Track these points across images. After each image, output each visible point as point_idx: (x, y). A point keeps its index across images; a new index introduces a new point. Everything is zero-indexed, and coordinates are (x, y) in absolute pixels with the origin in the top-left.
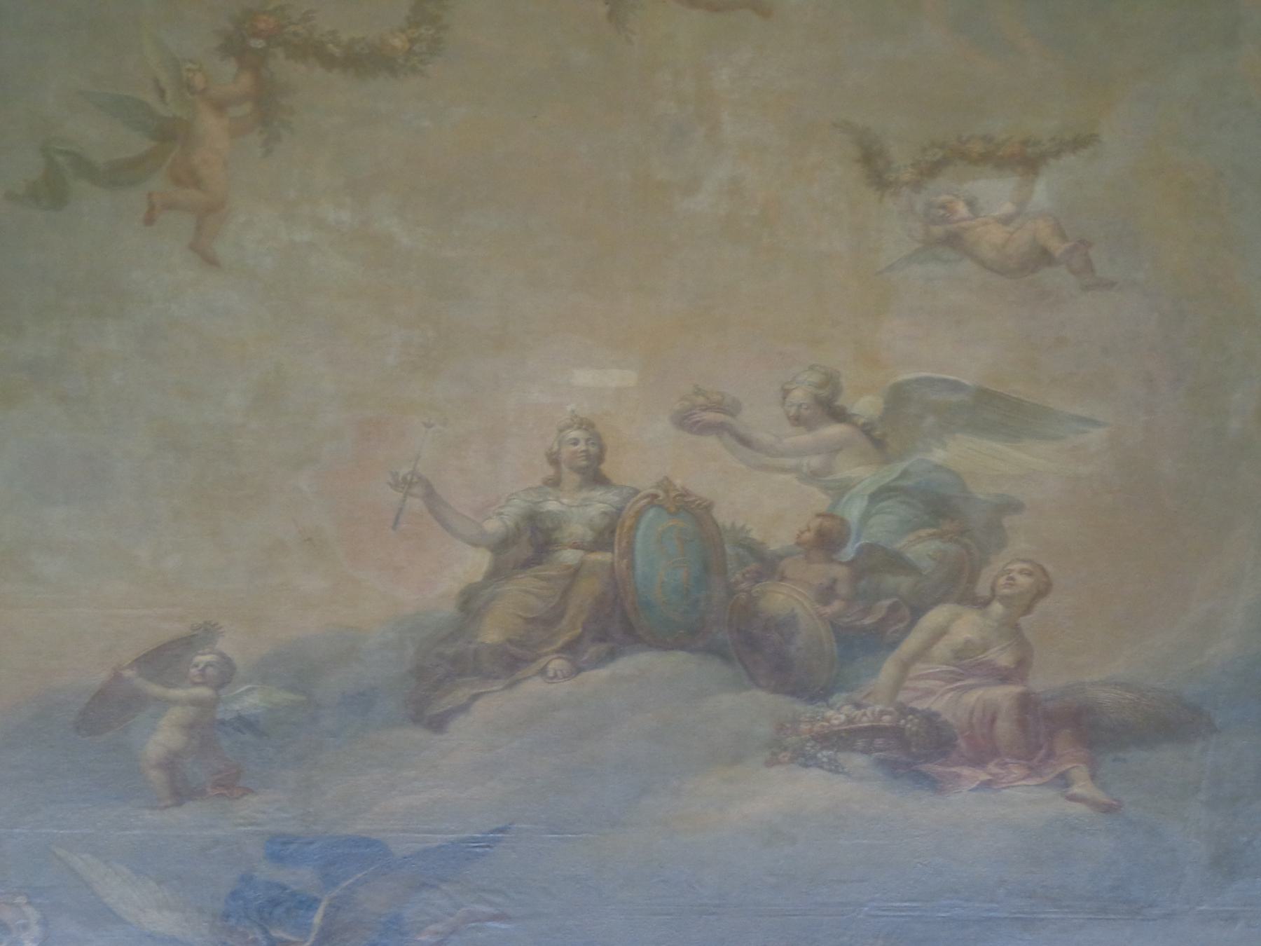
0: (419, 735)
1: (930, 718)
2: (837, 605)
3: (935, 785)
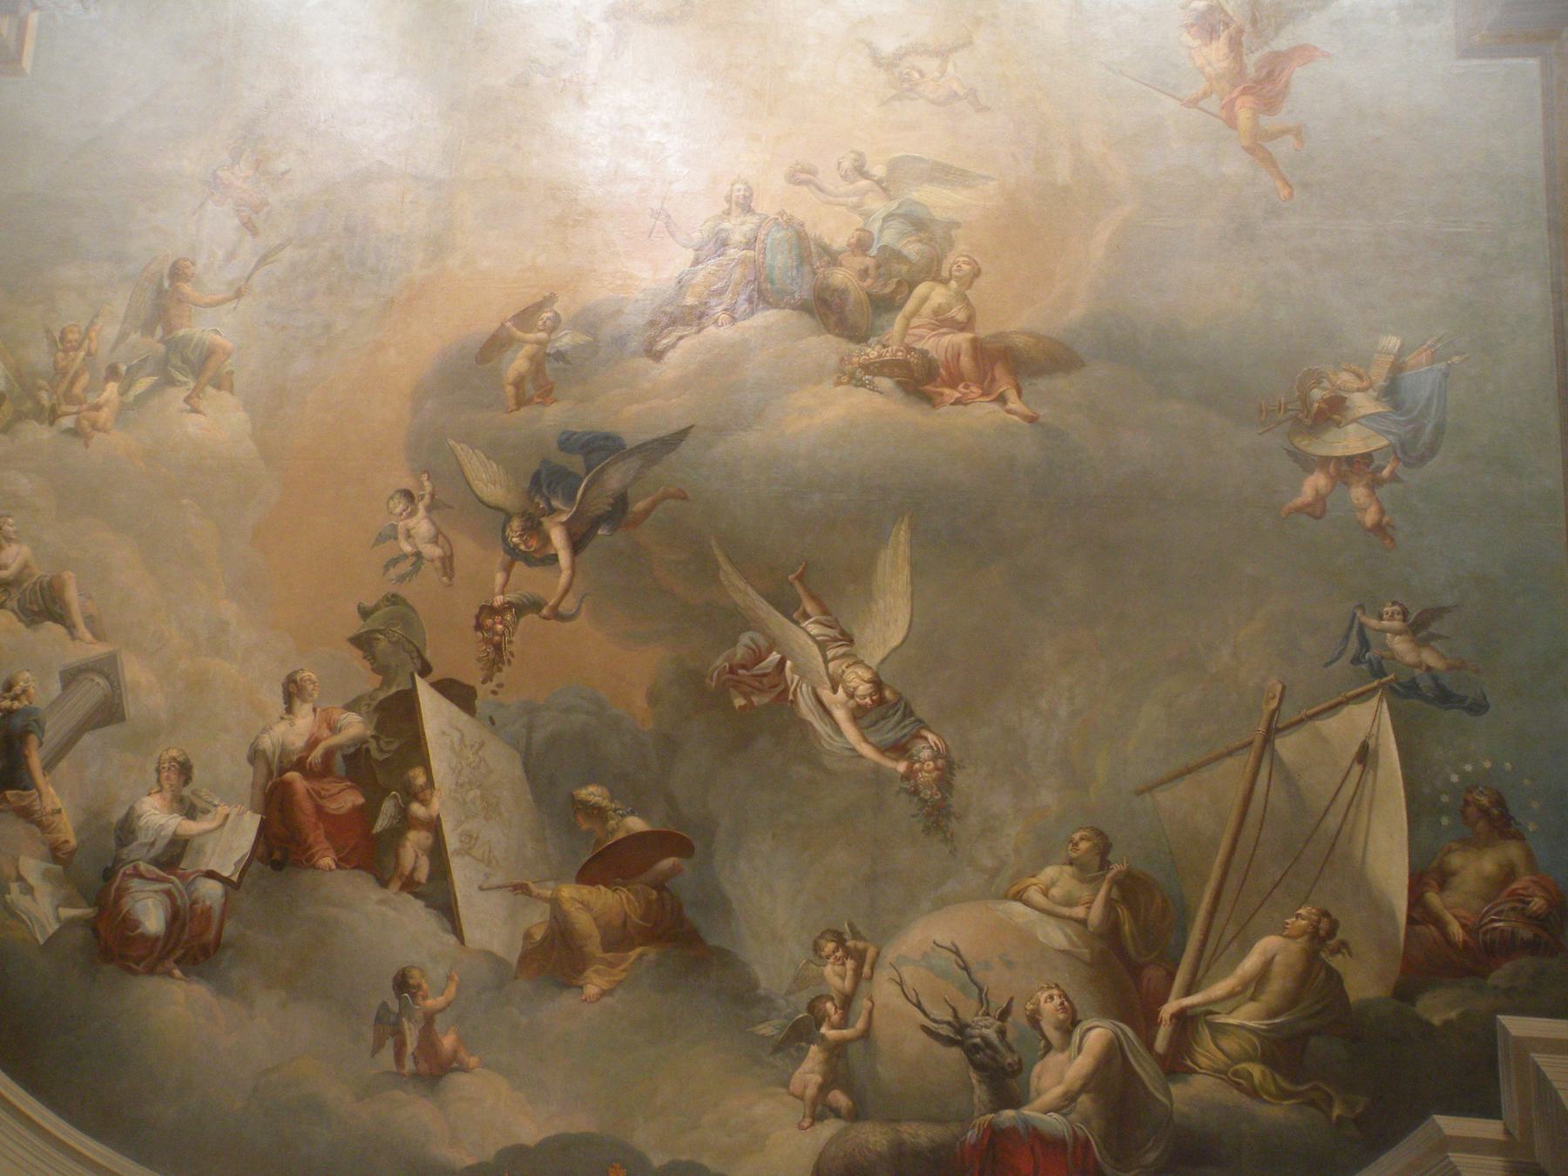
1: (924, 353)
2: (869, 281)
3: (930, 400)
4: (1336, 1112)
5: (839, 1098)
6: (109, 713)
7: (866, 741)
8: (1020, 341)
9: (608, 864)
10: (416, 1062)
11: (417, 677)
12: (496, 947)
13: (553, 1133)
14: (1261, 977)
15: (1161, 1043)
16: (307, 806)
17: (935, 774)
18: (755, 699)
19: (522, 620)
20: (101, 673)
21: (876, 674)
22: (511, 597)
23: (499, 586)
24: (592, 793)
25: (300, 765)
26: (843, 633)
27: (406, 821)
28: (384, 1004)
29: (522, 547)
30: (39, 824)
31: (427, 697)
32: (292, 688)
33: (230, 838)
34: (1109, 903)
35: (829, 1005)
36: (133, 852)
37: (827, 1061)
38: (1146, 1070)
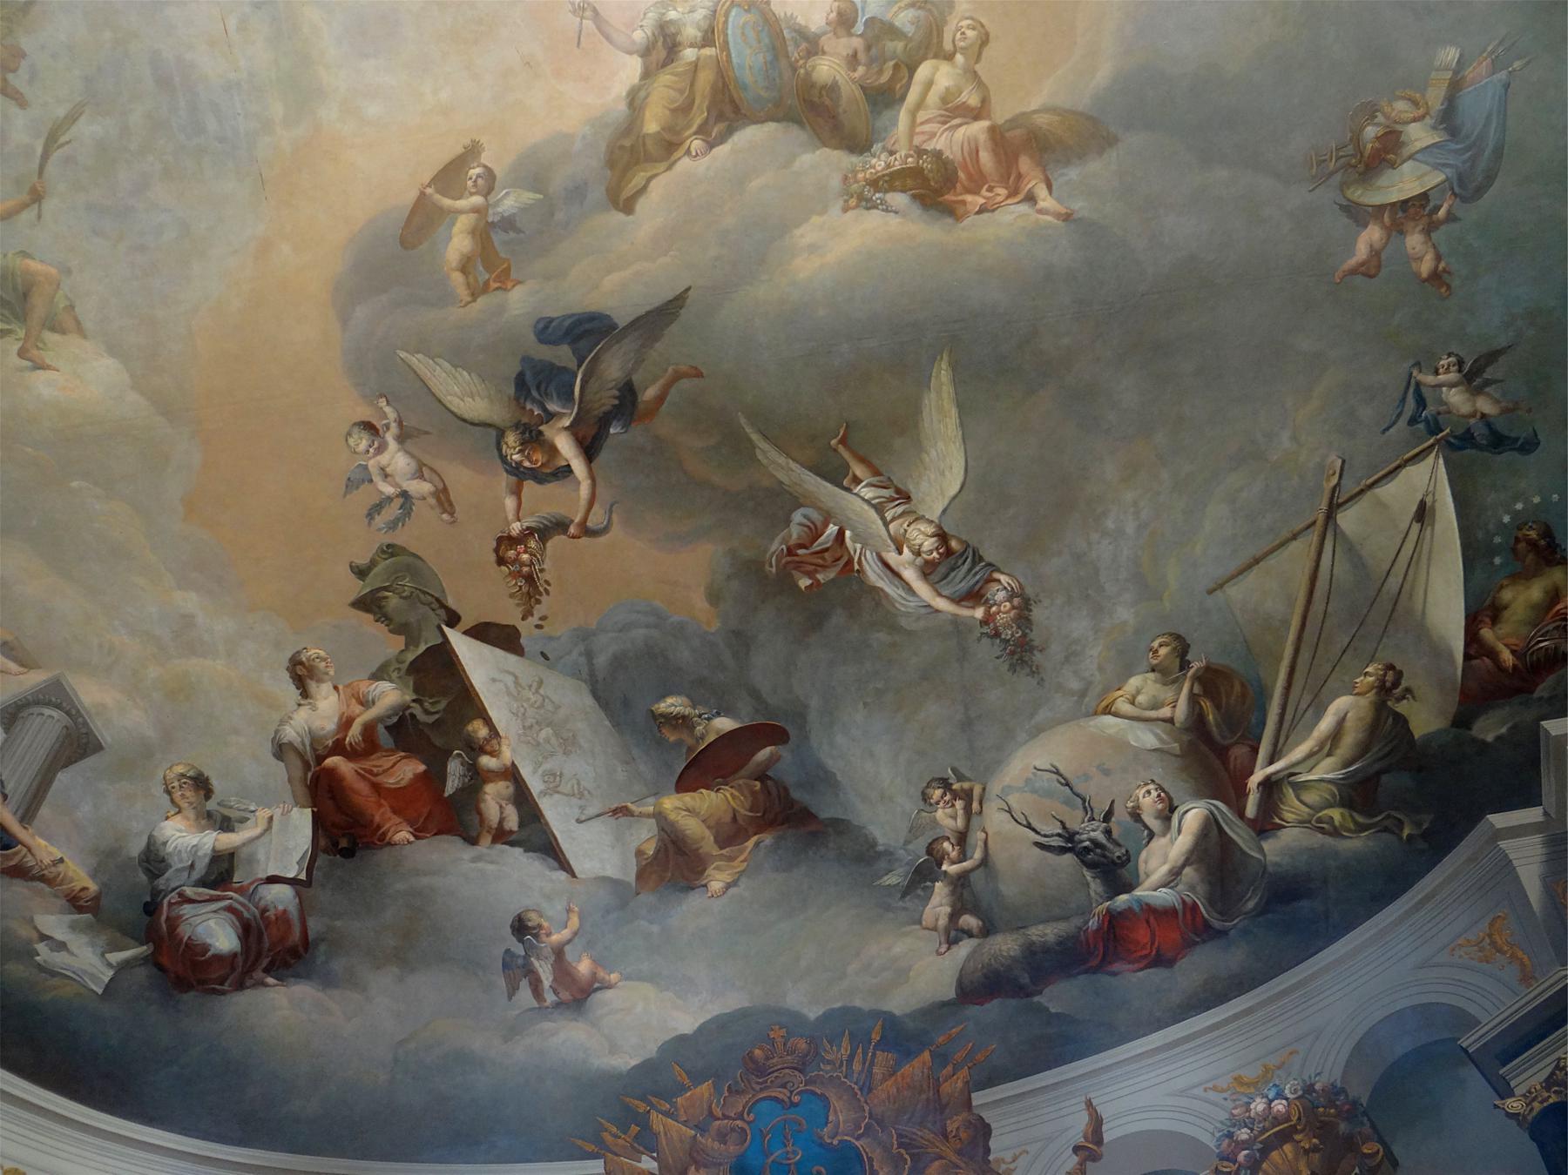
0: (621, 216)
1: (938, 154)
2: (861, 70)
3: (952, 212)
4: (1406, 832)
5: (969, 921)
6: (79, 744)
7: (940, 595)
8: (1042, 120)
9: (701, 770)
10: (556, 992)
11: (446, 629)
12: (611, 872)
13: (709, 1017)
14: (1336, 735)
15: (1251, 810)
16: (362, 787)
17: (1012, 613)
18: (820, 577)
19: (549, 544)
20: (48, 704)
21: (939, 527)
22: (529, 522)
23: (514, 512)
24: (673, 704)
25: (339, 748)
26: (898, 491)
27: (477, 778)
28: (508, 951)
29: (527, 464)
30: (42, 879)
31: (465, 648)
32: (300, 670)
33: (283, 839)
34: (1193, 698)
35: (946, 845)
36: (170, 879)
37: (953, 893)
38: (1240, 835)
